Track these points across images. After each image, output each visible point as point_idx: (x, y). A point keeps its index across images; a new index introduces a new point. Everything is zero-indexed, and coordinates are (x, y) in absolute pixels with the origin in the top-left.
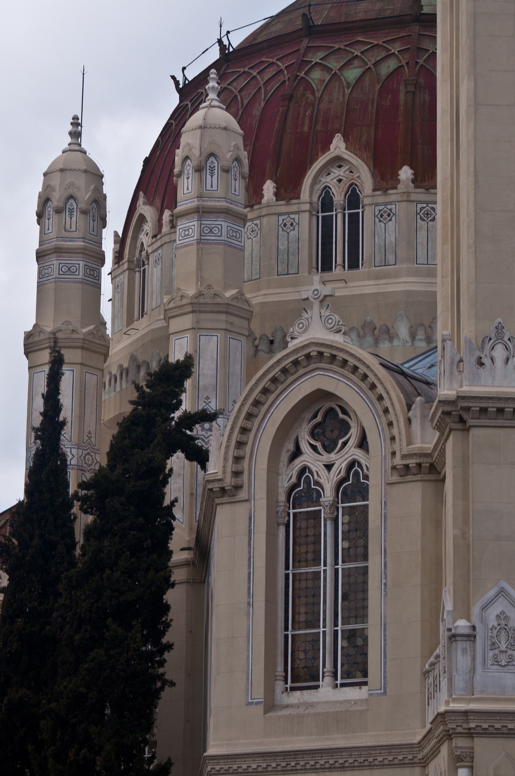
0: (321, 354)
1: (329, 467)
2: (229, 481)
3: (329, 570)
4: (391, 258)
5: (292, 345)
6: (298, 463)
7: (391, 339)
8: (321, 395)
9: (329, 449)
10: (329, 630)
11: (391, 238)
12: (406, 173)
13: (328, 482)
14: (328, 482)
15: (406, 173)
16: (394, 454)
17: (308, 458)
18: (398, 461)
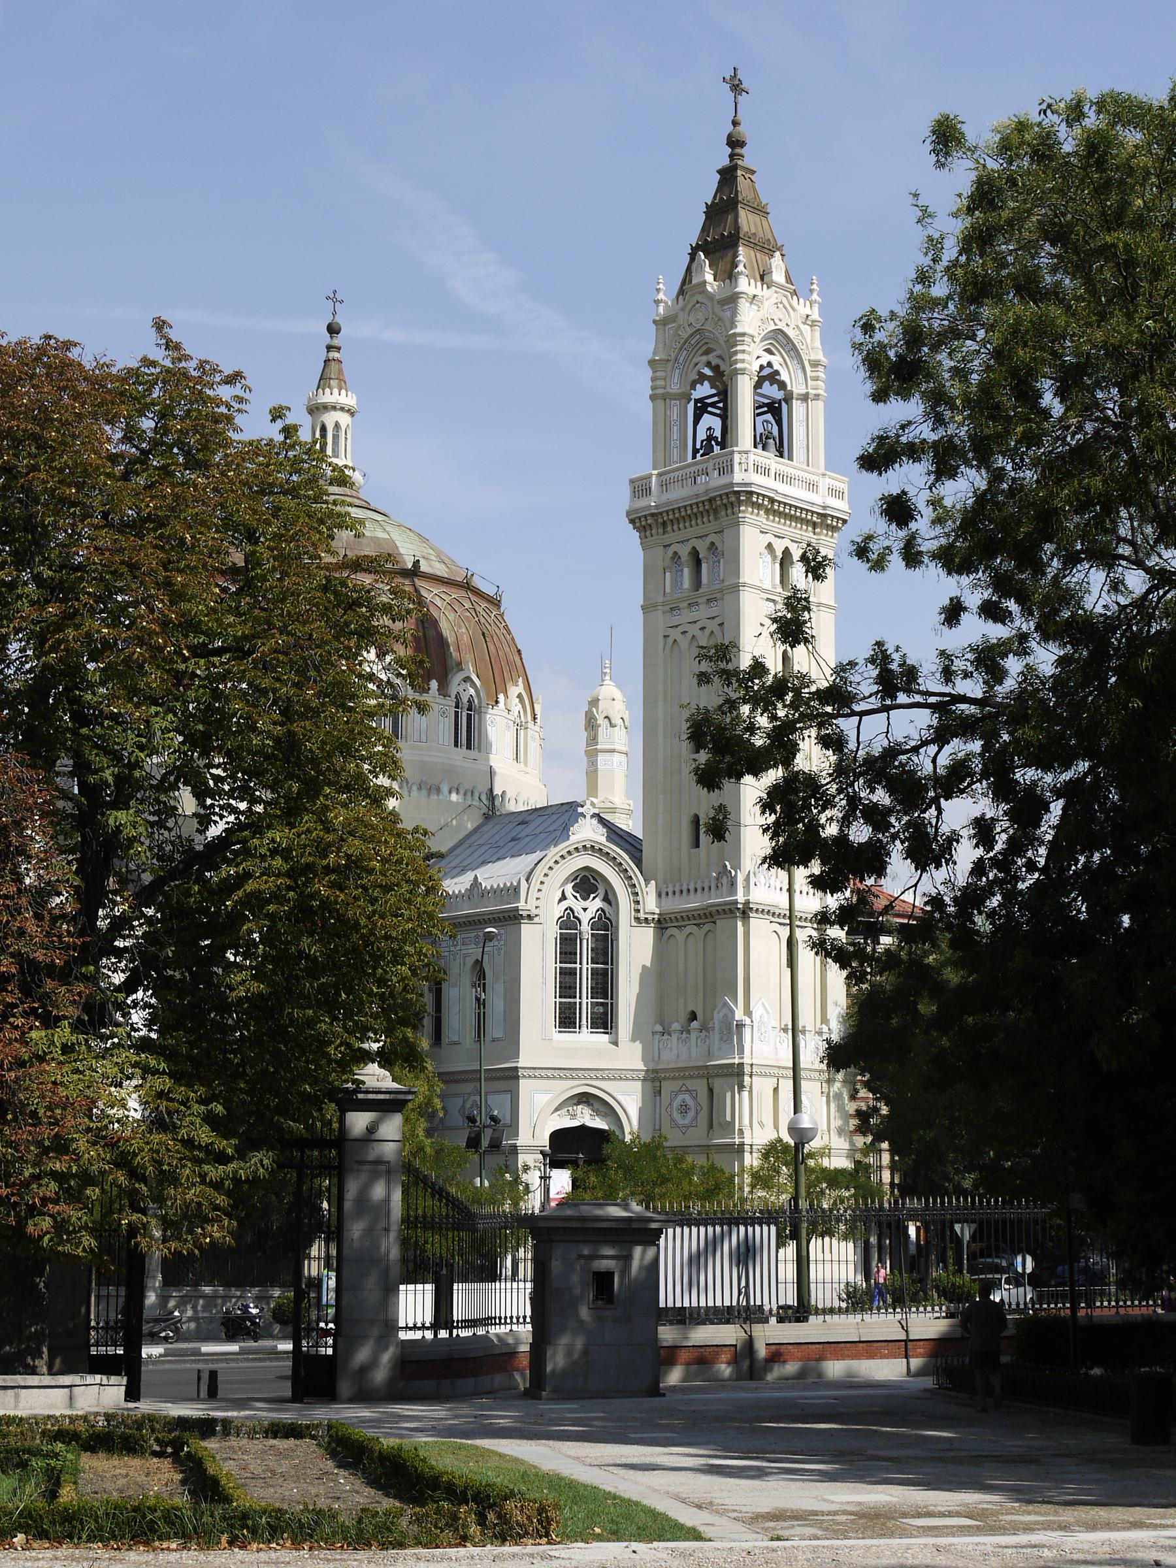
0: (592, 847)
1: (585, 910)
2: (534, 912)
3: (585, 967)
4: (424, 738)
5: (573, 839)
6: (565, 904)
7: (438, 795)
8: (587, 868)
9: (585, 899)
10: (584, 1001)
11: (424, 725)
12: (434, 684)
13: (585, 918)
14: (585, 918)
15: (434, 684)
16: (638, 911)
17: (570, 902)
18: (642, 916)
